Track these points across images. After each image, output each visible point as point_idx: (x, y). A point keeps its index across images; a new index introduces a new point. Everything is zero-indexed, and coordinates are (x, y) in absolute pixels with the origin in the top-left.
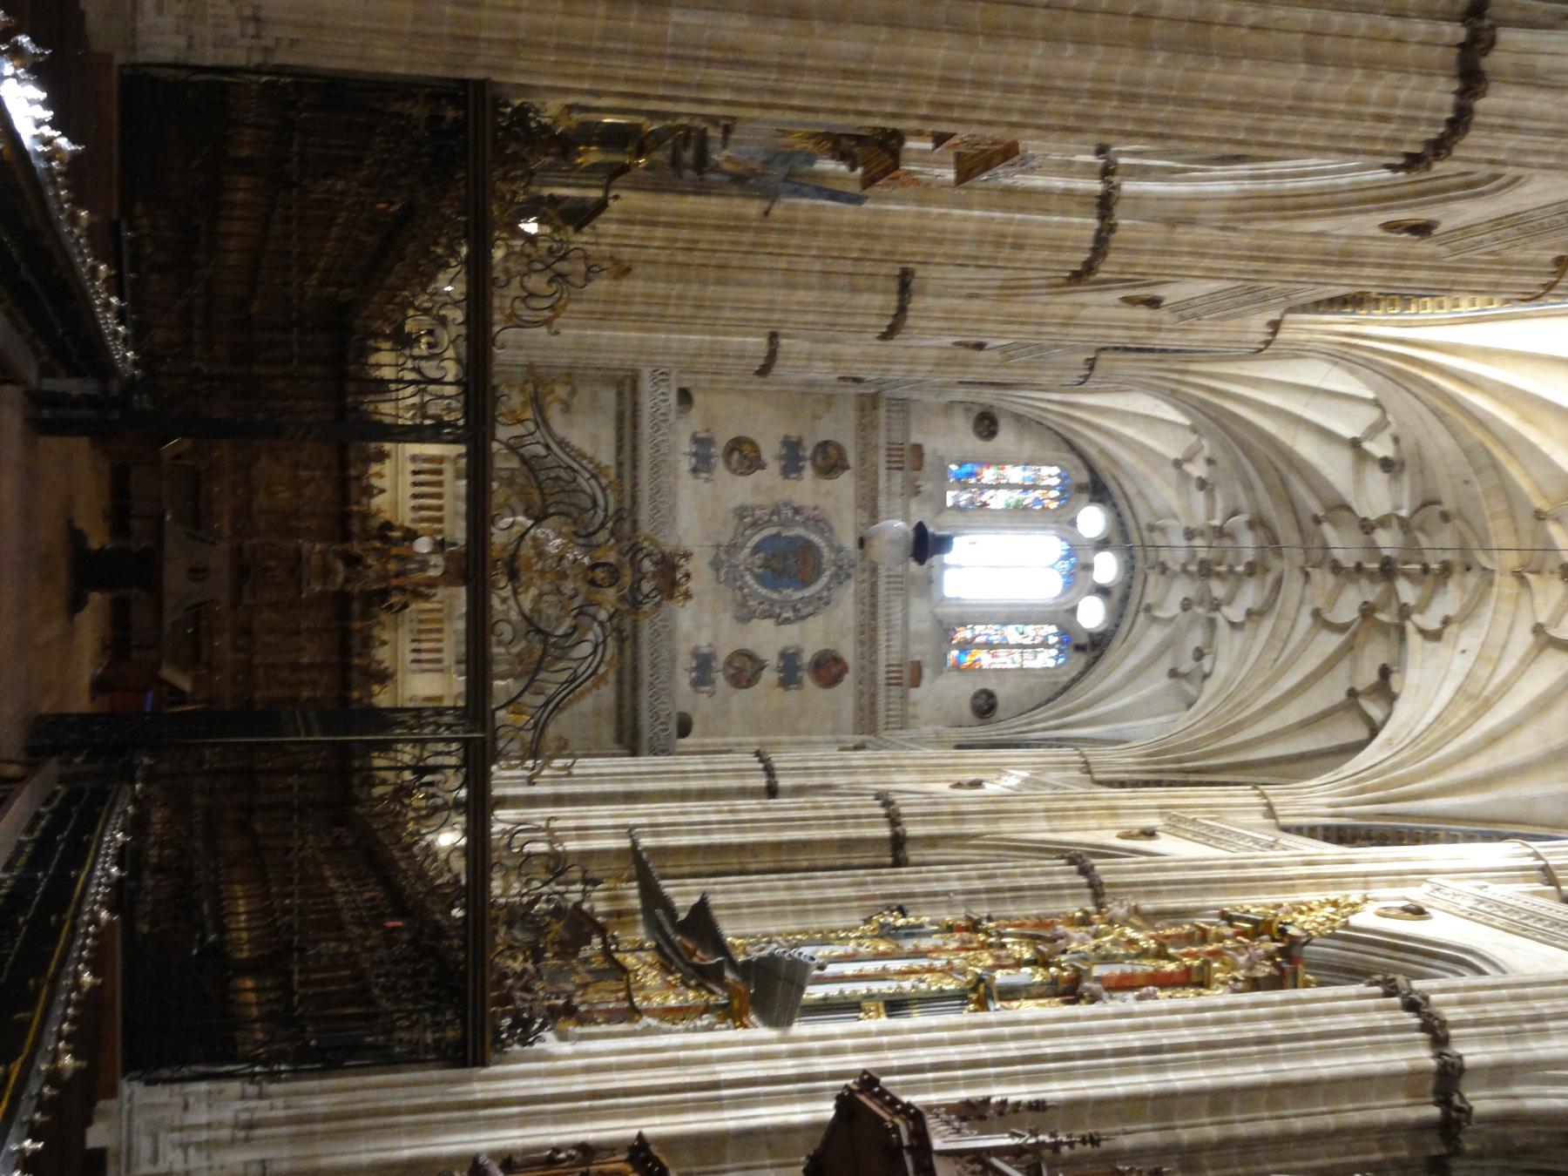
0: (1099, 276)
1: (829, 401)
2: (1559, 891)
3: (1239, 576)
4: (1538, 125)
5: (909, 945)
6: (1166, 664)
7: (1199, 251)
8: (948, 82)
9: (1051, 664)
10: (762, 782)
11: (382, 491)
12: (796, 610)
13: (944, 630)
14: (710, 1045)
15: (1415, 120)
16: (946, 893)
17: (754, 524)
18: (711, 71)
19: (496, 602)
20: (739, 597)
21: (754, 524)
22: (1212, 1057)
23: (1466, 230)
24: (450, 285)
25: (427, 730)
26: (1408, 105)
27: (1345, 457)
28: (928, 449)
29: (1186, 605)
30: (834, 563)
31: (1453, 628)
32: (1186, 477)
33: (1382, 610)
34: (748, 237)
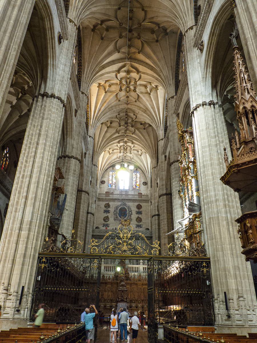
1: (98, 206)
3: (127, 146)
6: (139, 156)
10: (157, 217)
12: (130, 212)
13: (134, 189)
17: (117, 218)
21: (117, 218)
29: (131, 153)
31: (135, 114)
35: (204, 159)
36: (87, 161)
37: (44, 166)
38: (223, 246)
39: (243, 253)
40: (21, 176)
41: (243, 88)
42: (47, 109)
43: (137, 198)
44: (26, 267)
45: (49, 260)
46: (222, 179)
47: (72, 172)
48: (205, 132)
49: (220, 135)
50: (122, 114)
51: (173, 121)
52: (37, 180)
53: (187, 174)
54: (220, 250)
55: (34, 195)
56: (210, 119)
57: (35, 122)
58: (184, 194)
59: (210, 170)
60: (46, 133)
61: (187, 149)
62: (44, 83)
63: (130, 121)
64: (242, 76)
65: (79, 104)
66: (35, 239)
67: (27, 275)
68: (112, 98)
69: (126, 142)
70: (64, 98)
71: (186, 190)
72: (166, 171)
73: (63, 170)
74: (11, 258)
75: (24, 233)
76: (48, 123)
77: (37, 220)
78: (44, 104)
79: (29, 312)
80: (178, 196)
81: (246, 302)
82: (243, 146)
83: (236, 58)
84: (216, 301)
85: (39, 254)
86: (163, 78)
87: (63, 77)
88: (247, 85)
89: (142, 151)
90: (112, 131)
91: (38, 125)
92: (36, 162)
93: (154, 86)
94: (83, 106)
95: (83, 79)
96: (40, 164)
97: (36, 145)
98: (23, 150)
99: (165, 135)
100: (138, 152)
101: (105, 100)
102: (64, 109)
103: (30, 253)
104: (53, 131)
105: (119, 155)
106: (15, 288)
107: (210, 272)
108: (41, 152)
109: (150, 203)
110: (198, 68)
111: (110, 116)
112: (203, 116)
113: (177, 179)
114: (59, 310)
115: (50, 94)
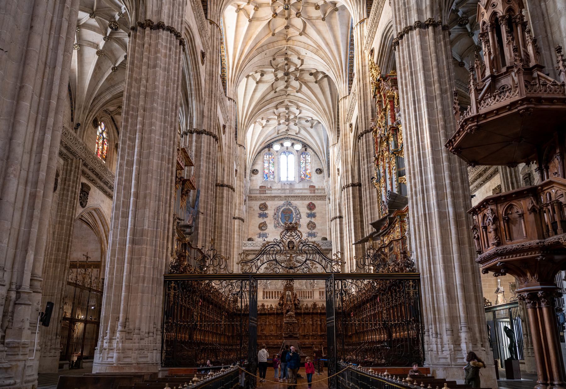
0: (217, 134)
1: (250, 207)
2: (366, 19)
4: (171, 10)
5: (382, 174)
6: (309, 129)
7: (210, 110)
8: (162, 159)
11: (271, 305)
14: (414, 217)
15: (170, 41)
16: (368, 168)
18: (160, 219)
19: (298, 272)
21: (278, 224)
22: (416, 87)
23: (203, 44)
24: (215, 284)
25: (332, 289)
26: (167, 43)
27: (261, 85)
28: (261, 185)
29: (296, 124)
31: (300, 57)
32: (266, 125)
34: (208, 218)
43: (307, 193)
63: (292, 69)
102: (182, 50)
115: (155, 23)
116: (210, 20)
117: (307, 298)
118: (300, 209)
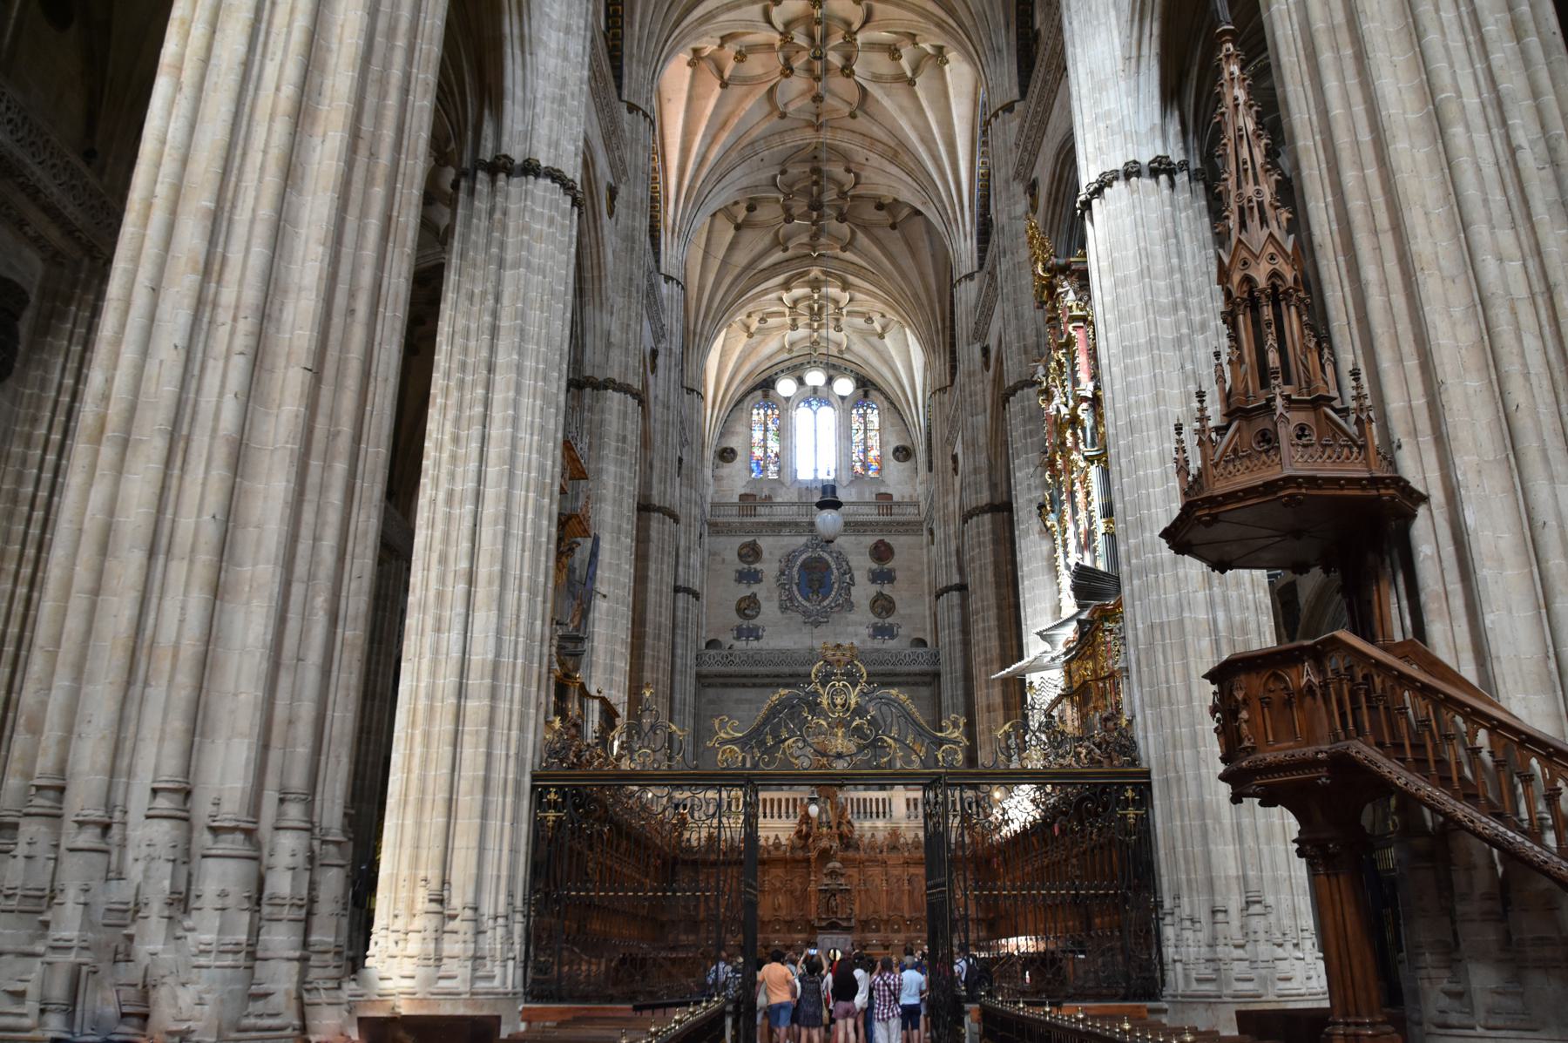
1: (712, 554)
3: (820, 297)
6: (875, 340)
9: (876, 412)
12: (845, 574)
13: (857, 479)
20: (837, 609)
23: (612, 166)
27: (748, 235)
28: (743, 492)
29: (839, 329)
30: (814, 550)
31: (852, 166)
32: (759, 330)
33: (841, 209)
35: (1133, 398)
36: (660, 382)
37: (522, 455)
38: (1198, 727)
39: (1224, 777)
40: (441, 496)
41: (1245, 201)
42: (511, 225)
43: (871, 514)
44: (494, 824)
45: (569, 795)
46: (1166, 534)
47: (613, 444)
48: (1135, 288)
49: (1193, 301)
50: (794, 171)
51: (1012, 209)
52: (502, 508)
53: (1069, 445)
54: (1186, 741)
55: (497, 568)
56: (1156, 233)
57: (473, 280)
58: (1060, 521)
59: (1154, 443)
60: (519, 322)
61: (1069, 343)
62: (491, 114)
64: (1245, 153)
65: (622, 161)
66: (515, 725)
67: (501, 850)
68: (750, 110)
69: (815, 285)
70: (572, 168)
71: (1067, 507)
72: (989, 411)
73: (582, 447)
74: (442, 795)
75: (476, 706)
76: (522, 282)
77: (515, 658)
78: (499, 205)
79: (520, 972)
80: (1035, 525)
81: (1272, 918)
82: (1234, 425)
83: (1226, 75)
84: (1168, 919)
85: (535, 777)
86: (968, 22)
87: (564, 84)
88: (1258, 192)
89: (888, 316)
90: (755, 241)
91: (484, 294)
92: (493, 443)
93: (930, 50)
94: (636, 167)
95: (630, 47)
96: (507, 448)
97: (485, 372)
98: (439, 395)
99: (982, 259)
100: (869, 320)
101: (721, 119)
102: (575, 217)
103: (502, 775)
104: (542, 312)
105: (790, 336)
106: (464, 894)
107: (1148, 818)
108: (506, 399)
109: (926, 537)
110: (1107, 13)
111: (745, 182)
112: (1128, 221)
113: (1034, 456)
114: (623, 961)
115: (518, 161)
116: (628, 102)
117: (874, 816)
118: (850, 558)
